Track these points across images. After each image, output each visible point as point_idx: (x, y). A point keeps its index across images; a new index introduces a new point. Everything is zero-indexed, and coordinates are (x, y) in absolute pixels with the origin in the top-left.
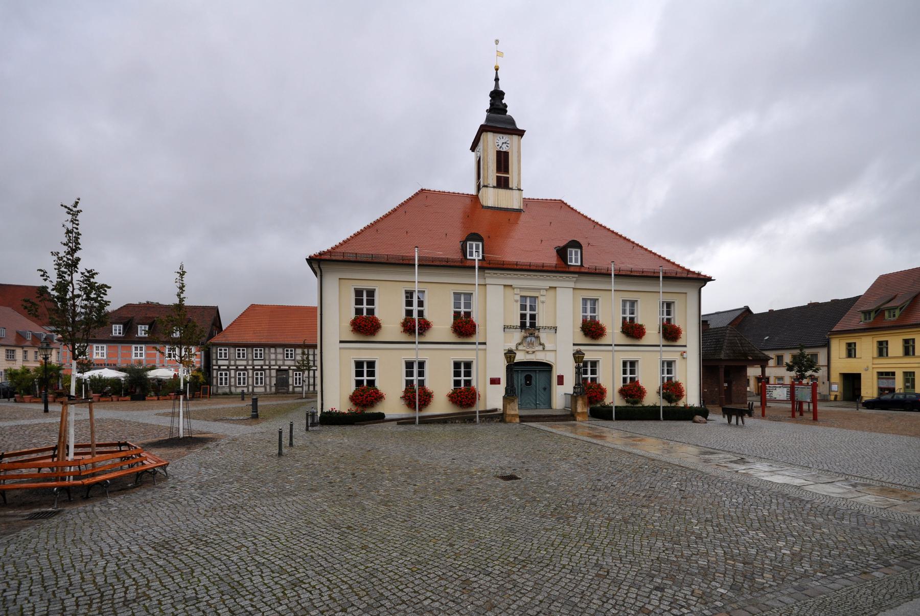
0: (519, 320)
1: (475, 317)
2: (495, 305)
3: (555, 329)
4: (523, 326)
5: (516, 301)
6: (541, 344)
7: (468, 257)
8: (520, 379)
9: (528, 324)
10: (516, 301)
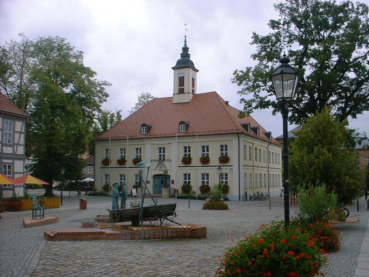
0: (159, 157)
2: (149, 152)
3: (171, 160)
4: (160, 159)
5: (156, 150)
8: (158, 181)
10: (156, 150)
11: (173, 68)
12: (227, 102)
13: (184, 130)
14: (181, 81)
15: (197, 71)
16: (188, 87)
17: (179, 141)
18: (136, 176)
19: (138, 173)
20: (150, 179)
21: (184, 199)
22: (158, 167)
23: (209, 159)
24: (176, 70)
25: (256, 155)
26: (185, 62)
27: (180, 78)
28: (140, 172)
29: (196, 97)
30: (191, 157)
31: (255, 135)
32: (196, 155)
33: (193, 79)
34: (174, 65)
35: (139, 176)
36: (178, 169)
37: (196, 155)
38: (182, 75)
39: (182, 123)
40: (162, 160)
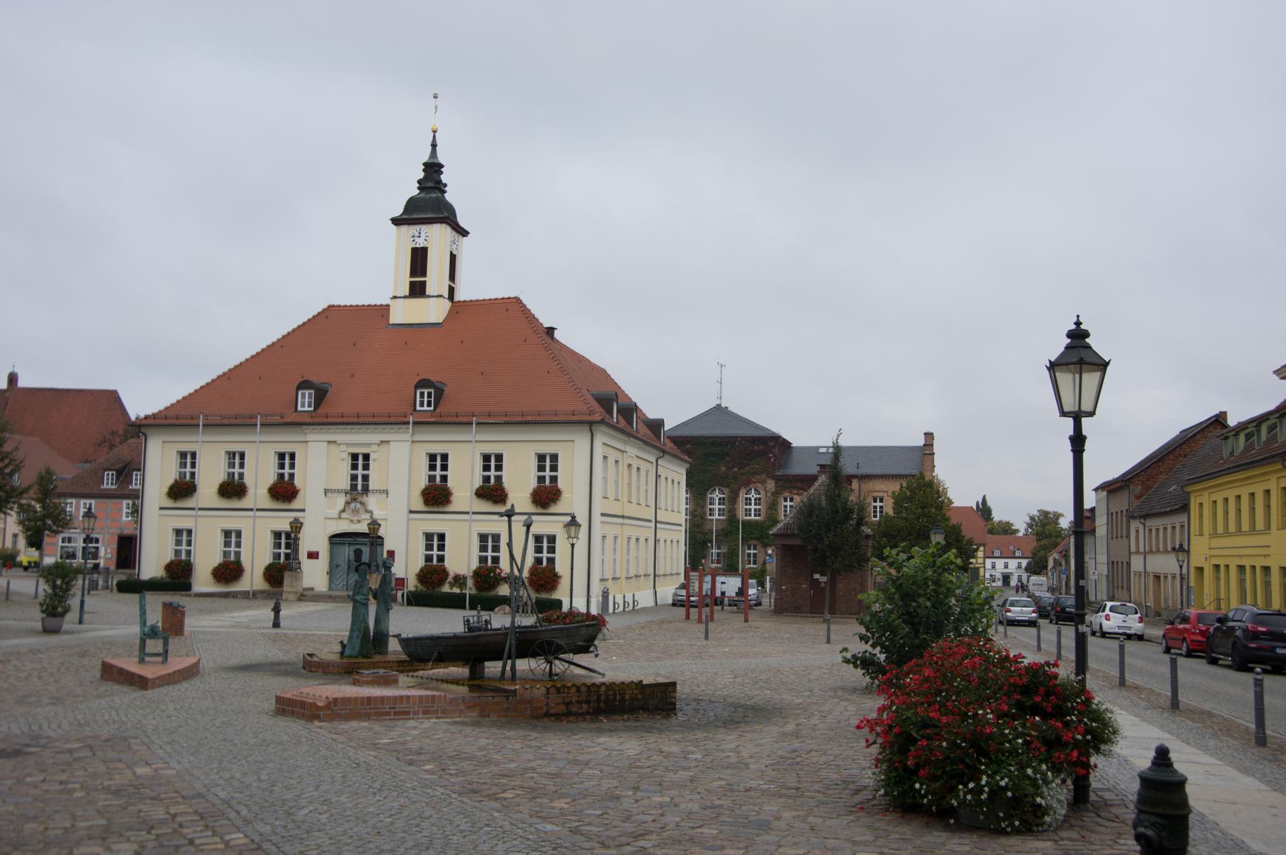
1: (297, 482)
2: (321, 462)
3: (386, 492)
4: (354, 487)
6: (367, 511)
7: (299, 408)
8: (347, 552)
9: (359, 487)
11: (397, 221)
12: (550, 331)
13: (429, 405)
14: (419, 259)
15: (464, 233)
16: (436, 278)
17: (417, 438)
18: (277, 535)
19: (284, 526)
20: (323, 548)
21: (426, 609)
22: (349, 511)
23: (503, 490)
24: (405, 229)
25: (629, 485)
26: (430, 204)
27: (414, 251)
28: (297, 526)
29: (459, 308)
30: (449, 484)
31: (623, 423)
32: (464, 478)
33: (453, 258)
34: (398, 211)
35: (289, 539)
36: (409, 520)
37: (464, 478)
38: (420, 243)
39: (423, 383)
40: (358, 489)
